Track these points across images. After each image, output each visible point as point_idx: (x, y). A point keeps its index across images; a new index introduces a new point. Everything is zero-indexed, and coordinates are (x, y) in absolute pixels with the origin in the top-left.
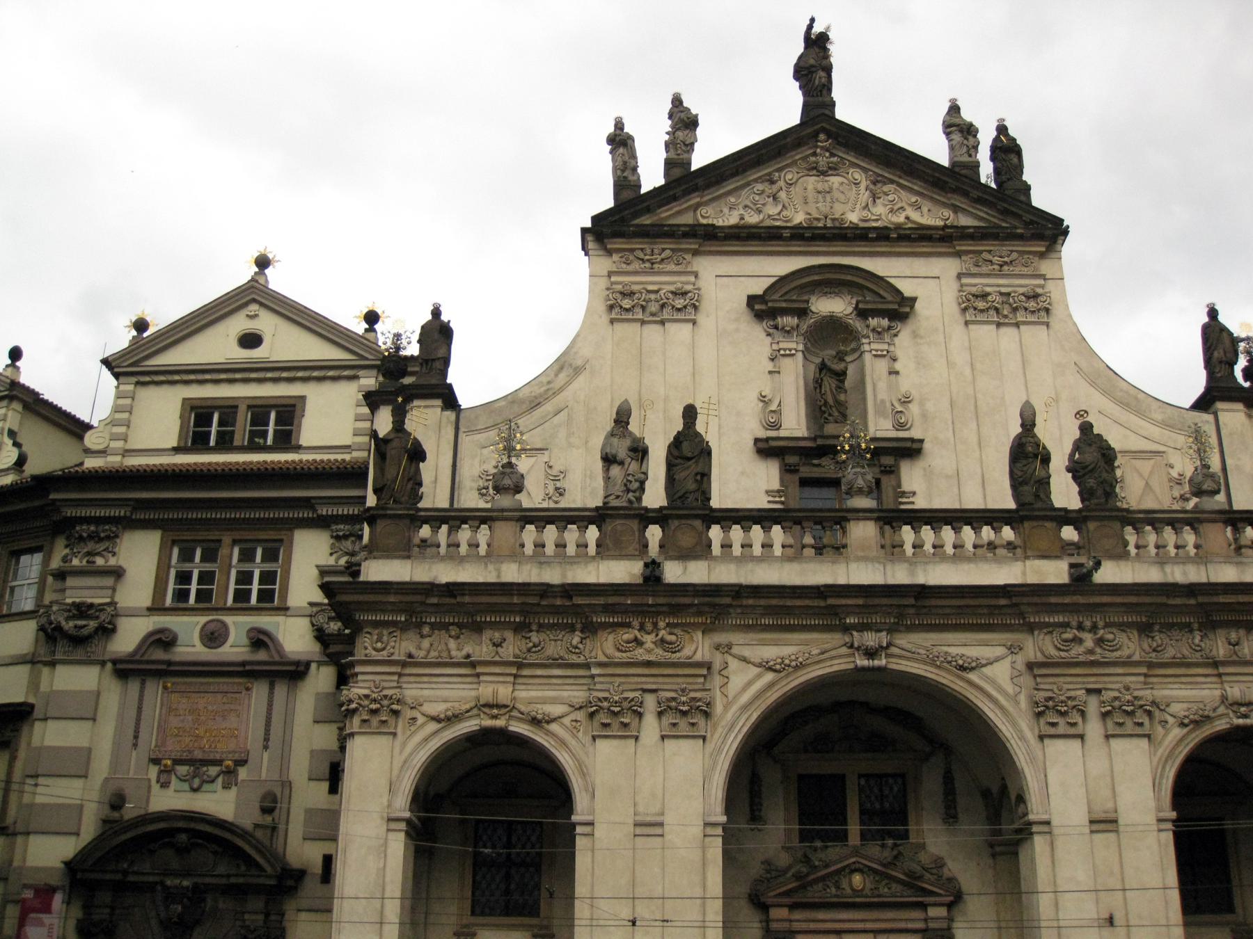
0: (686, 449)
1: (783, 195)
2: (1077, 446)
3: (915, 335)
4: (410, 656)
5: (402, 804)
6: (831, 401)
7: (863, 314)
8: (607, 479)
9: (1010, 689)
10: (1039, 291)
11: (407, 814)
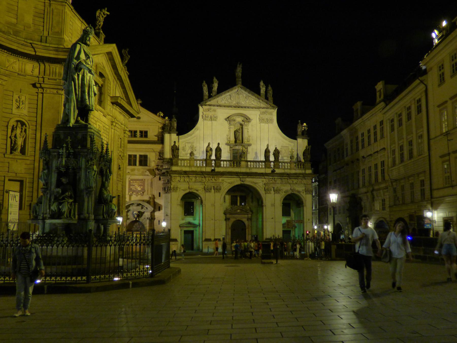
0: (218, 150)
1: (232, 98)
2: (275, 151)
3: (252, 125)
4: (179, 181)
6: (238, 137)
7: (244, 122)
9: (262, 187)
11: (180, 204)
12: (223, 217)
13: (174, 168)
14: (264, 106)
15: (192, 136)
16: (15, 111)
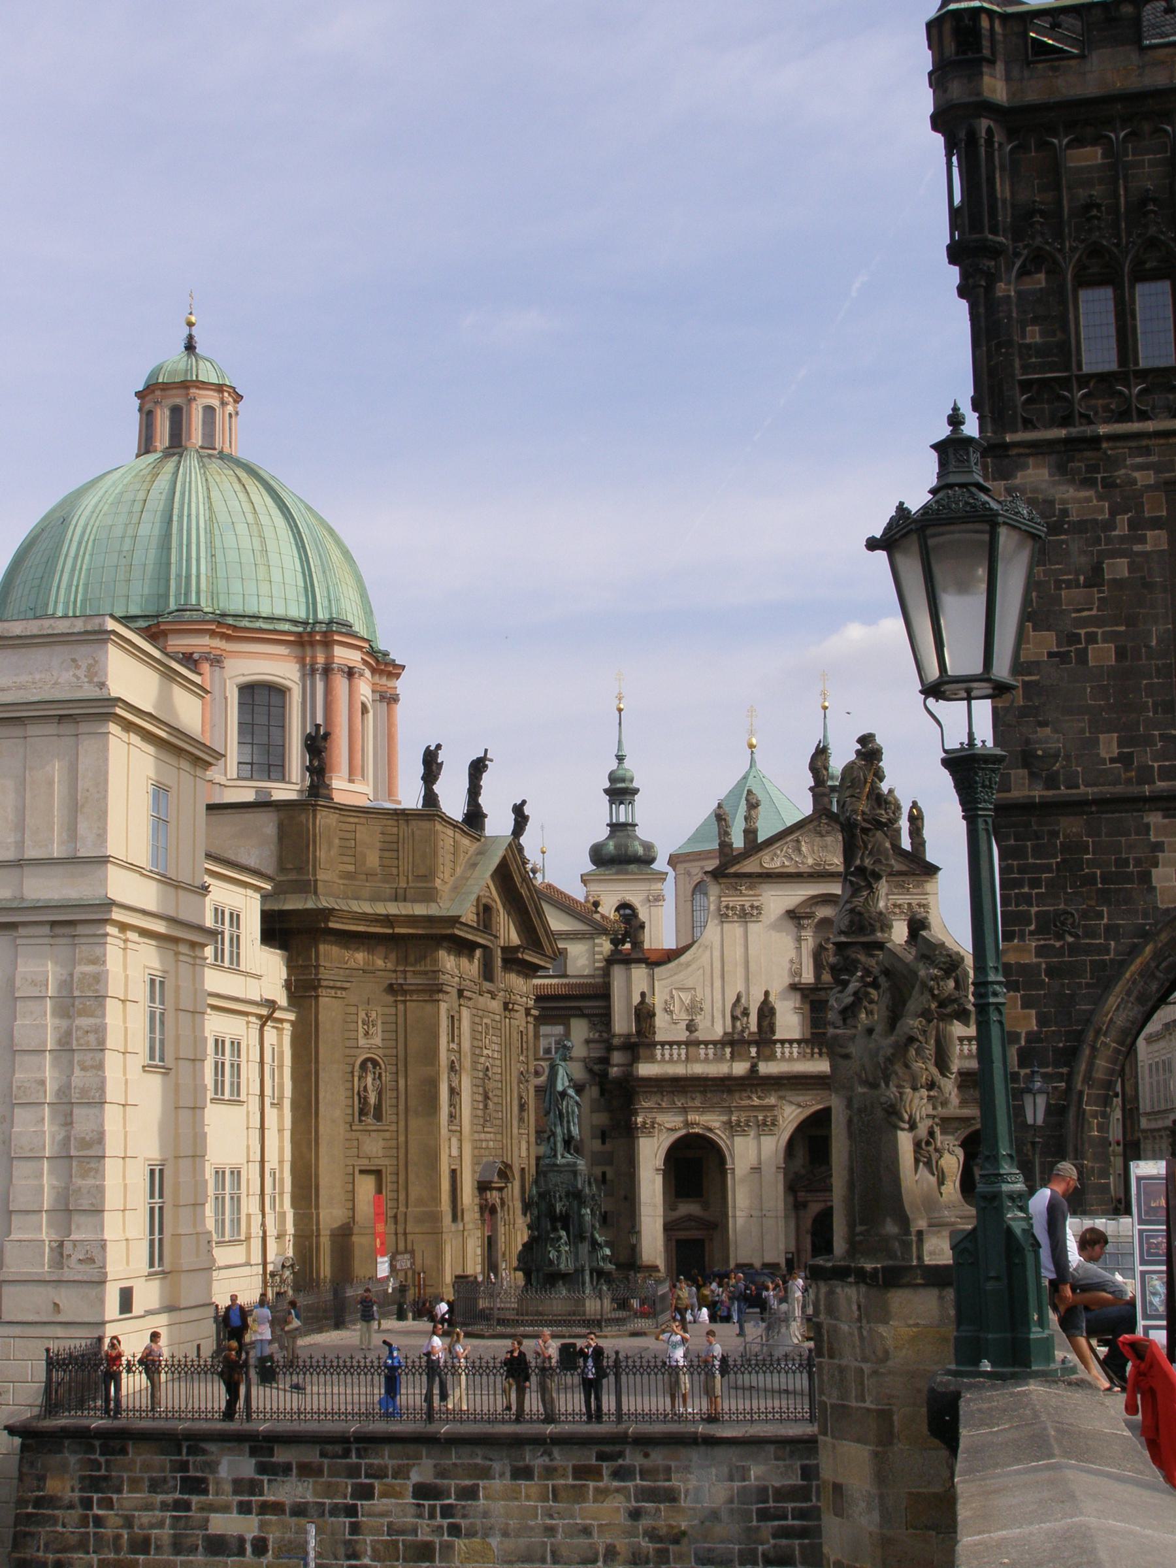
0: (766, 1009)
5: (659, 1162)
8: (734, 1026)
10: (924, 902)
12: (791, 1199)
13: (645, 1069)
14: (904, 868)
15: (690, 969)
16: (362, 1042)
